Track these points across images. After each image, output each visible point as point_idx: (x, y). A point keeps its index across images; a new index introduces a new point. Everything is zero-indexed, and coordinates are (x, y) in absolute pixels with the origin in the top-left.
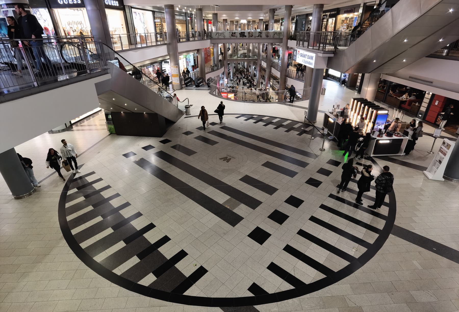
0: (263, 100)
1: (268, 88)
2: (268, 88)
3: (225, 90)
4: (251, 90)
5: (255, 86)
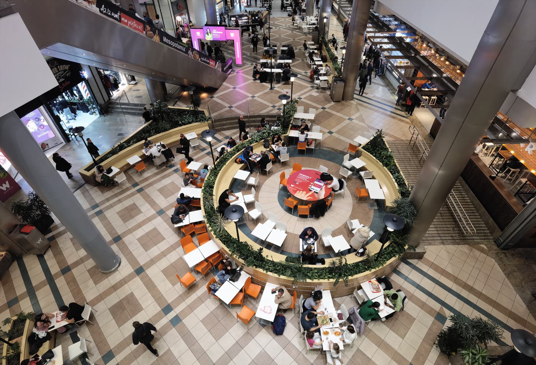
0: (313, 45)
1: (325, 15)
2: (325, 15)
4: (293, 20)
5: (304, 11)
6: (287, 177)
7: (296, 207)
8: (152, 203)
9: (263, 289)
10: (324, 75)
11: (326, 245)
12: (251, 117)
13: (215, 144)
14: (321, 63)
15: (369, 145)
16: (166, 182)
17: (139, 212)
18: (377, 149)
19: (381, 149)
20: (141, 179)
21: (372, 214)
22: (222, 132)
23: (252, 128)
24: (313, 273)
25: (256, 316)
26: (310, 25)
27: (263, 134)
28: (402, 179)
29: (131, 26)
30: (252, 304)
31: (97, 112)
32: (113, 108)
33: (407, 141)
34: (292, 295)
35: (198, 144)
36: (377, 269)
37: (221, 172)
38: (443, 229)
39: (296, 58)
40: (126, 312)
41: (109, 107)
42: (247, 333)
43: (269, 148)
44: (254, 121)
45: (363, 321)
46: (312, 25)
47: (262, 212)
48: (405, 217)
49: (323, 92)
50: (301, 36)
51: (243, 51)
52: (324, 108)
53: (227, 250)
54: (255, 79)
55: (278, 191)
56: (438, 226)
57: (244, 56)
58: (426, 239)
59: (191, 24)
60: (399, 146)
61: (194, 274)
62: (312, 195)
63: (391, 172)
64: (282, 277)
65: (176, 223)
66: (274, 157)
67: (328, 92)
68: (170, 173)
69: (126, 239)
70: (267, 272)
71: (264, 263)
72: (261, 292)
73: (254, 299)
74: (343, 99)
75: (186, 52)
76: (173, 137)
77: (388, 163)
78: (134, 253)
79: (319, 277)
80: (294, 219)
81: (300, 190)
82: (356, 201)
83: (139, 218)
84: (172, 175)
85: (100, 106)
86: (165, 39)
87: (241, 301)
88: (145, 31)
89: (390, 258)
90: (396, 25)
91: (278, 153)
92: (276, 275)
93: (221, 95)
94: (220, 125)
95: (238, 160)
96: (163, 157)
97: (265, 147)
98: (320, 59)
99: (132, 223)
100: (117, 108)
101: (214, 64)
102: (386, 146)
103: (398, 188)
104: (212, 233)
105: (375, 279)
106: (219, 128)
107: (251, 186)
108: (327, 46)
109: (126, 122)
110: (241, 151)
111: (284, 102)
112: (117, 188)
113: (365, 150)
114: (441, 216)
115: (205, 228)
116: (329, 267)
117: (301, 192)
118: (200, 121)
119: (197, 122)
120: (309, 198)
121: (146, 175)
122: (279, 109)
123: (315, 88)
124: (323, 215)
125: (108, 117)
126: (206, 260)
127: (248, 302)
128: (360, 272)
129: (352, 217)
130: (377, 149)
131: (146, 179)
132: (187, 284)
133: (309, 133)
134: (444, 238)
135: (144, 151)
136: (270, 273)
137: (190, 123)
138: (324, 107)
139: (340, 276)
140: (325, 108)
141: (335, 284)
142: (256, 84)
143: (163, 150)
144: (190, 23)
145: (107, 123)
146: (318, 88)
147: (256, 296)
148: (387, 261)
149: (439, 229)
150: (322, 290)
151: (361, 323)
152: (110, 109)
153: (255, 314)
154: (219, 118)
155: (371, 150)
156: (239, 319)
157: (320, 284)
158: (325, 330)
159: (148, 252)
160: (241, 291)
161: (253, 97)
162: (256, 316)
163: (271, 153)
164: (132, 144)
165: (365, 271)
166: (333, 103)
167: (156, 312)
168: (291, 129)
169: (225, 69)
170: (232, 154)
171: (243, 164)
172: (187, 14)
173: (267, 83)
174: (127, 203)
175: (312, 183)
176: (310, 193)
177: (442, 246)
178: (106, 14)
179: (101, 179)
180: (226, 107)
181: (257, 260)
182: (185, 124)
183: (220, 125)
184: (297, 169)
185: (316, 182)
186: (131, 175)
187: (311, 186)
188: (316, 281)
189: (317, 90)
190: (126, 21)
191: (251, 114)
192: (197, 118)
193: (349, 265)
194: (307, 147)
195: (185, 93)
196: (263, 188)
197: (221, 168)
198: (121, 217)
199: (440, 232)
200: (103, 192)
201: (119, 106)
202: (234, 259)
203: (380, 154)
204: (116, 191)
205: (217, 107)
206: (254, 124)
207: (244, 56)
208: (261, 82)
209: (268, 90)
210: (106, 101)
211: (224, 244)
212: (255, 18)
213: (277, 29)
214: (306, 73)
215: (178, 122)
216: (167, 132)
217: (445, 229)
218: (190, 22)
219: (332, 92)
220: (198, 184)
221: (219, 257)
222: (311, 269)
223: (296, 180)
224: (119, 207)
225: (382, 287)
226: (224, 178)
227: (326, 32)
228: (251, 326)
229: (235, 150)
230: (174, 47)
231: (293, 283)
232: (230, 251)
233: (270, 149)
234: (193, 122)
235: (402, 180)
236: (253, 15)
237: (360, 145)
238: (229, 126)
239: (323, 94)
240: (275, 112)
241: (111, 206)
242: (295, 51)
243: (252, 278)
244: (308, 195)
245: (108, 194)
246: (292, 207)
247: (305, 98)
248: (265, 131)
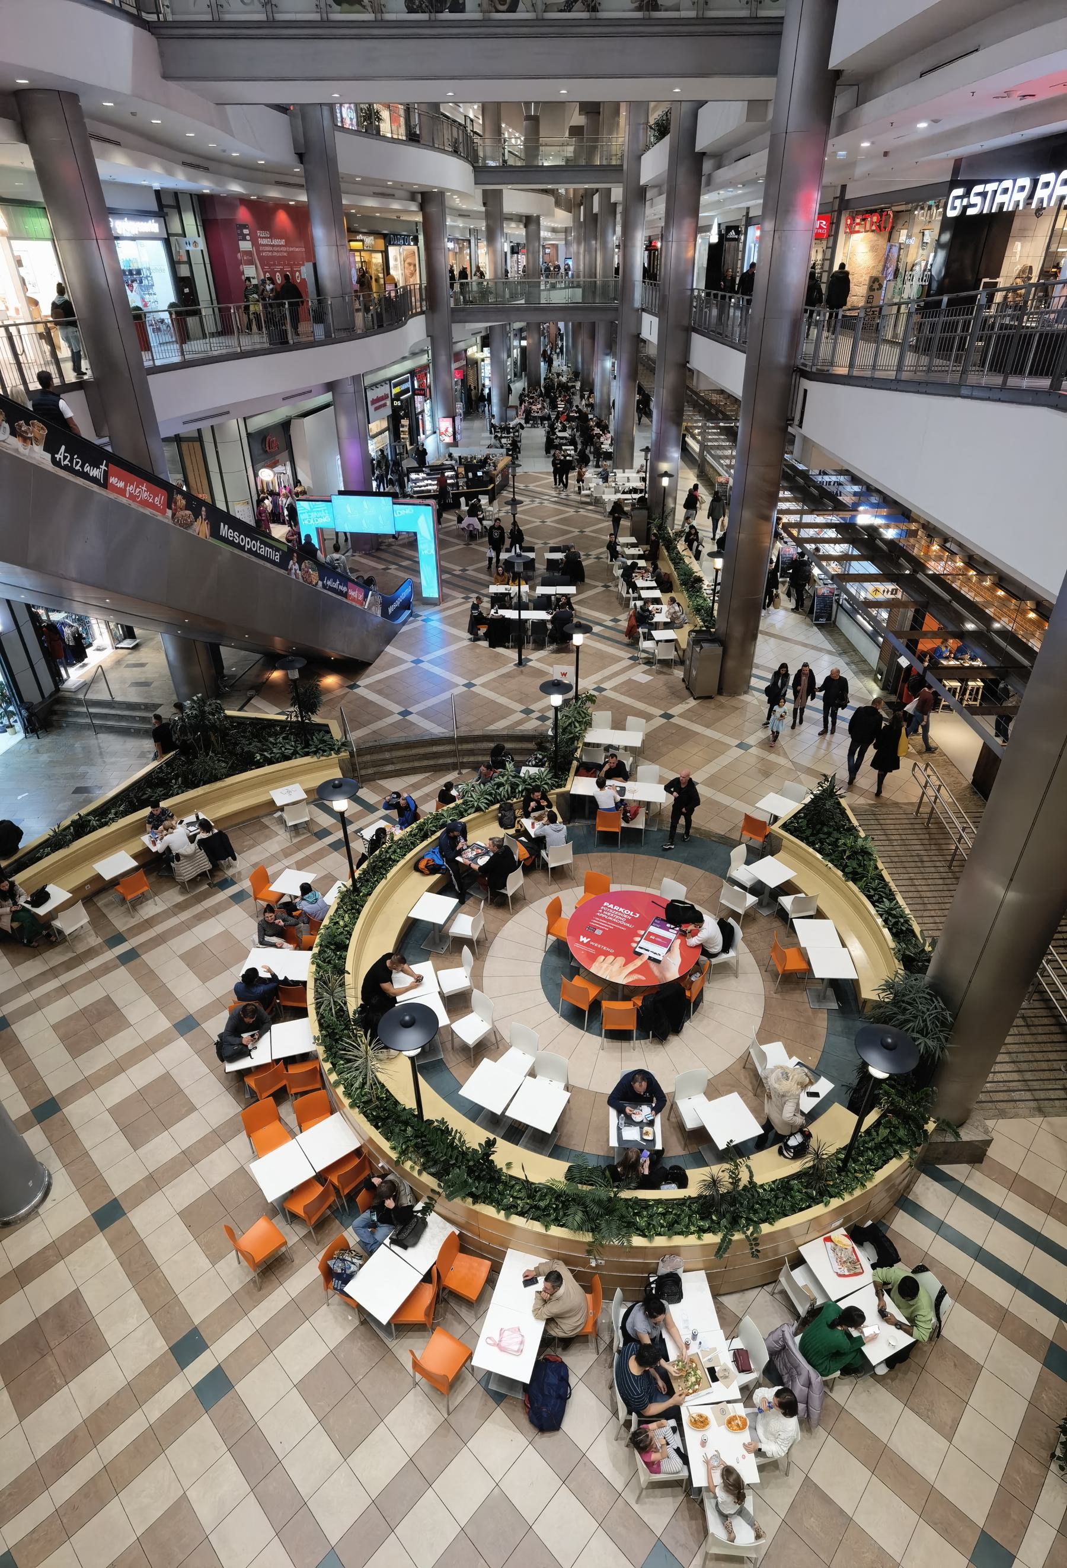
0: (633, 545)
1: (664, 466)
2: (664, 466)
3: (424, 479)
5: (608, 456)
6: (568, 912)
7: (595, 1006)
8: (163, 997)
9: (495, 1270)
10: (667, 626)
11: (690, 1124)
12: (463, 740)
13: (358, 816)
14: (657, 594)
15: (800, 818)
16: (208, 930)
17: (121, 1022)
18: (826, 829)
19: (838, 830)
20: (133, 922)
21: (822, 1023)
22: (381, 782)
23: (464, 771)
24: (651, 1217)
25: (475, 1362)
26: (624, 493)
27: (498, 788)
28: (902, 917)
29: (132, 497)
30: (461, 1321)
31: (18, 726)
32: (65, 714)
33: (911, 807)
34: (588, 1289)
35: (307, 819)
36: (848, 1198)
37: (371, 900)
38: (1035, 1065)
39: (587, 580)
40: (49, 1360)
41: (55, 713)
42: (446, 1426)
43: (513, 826)
44: (472, 753)
45: (816, 1379)
46: (630, 492)
47: (493, 1022)
48: (919, 1032)
49: (665, 673)
50: (599, 521)
51: (443, 563)
52: (667, 716)
53: (385, 1145)
54: (476, 638)
55: (540, 956)
56: (1021, 1057)
57: (445, 576)
58: (988, 1099)
59: (299, 489)
60: (888, 822)
61: (279, 1222)
62: (643, 969)
63: (869, 897)
64: (556, 1231)
65: (232, 1059)
66: (527, 855)
67: (679, 673)
68: (219, 903)
69: (74, 1112)
70: (507, 1216)
71: (500, 1187)
72: (491, 1281)
73: (468, 1303)
74: (720, 692)
75: (283, 564)
76: (235, 798)
77: (860, 870)
78: (95, 1156)
79: (672, 1229)
80: (592, 1043)
81: (606, 954)
82: (773, 987)
83: (120, 1044)
84: (225, 909)
85: (27, 709)
86: (224, 530)
87: (427, 1314)
88: (170, 507)
89: (886, 1162)
90: (855, 494)
91: (538, 843)
92: (537, 1227)
93: (379, 681)
94: (375, 764)
95: (422, 865)
96: (202, 854)
97: (503, 825)
98: (654, 584)
99: (99, 1058)
100: (78, 714)
101: (361, 597)
102: (850, 822)
103: (892, 944)
104: (340, 1090)
105: (842, 1231)
106: (370, 771)
107: (460, 942)
108: (670, 545)
109: (101, 754)
110: (434, 837)
111: (556, 700)
112: (58, 949)
113: (791, 834)
114: (1028, 1026)
115: (318, 1074)
116: (700, 1197)
117: (611, 958)
118: (315, 753)
119: (307, 754)
120: (636, 977)
121: (151, 909)
122: (543, 718)
123: (641, 661)
124: (677, 1029)
125: (47, 741)
126: (321, 1177)
127: (449, 1316)
128: (795, 1209)
129: (766, 1035)
130: (826, 829)
131: (149, 923)
132: (259, 1257)
133: (628, 785)
134: (1042, 1095)
135: (146, 839)
136: (517, 1220)
137: (287, 758)
138: (670, 712)
139: (734, 1223)
140: (672, 716)
141: (721, 1249)
142: (478, 651)
143: (203, 835)
144: (296, 486)
145: (44, 757)
146: (649, 662)
147: (473, 1295)
148: (876, 1170)
149: (1024, 1066)
150: (680, 1272)
151: (809, 1384)
152: (55, 718)
153: (470, 1357)
154: (371, 744)
155: (809, 832)
156: (418, 1376)
157: (674, 1251)
158: (696, 1411)
159: (141, 1151)
160: (427, 1278)
161: (469, 685)
162: (475, 1362)
163: (521, 842)
164: (113, 820)
165: (809, 1207)
166: (692, 703)
167: (149, 1359)
168: (577, 774)
169: (391, 610)
170: (405, 846)
171: (438, 876)
172: (288, 463)
173: (508, 648)
174: (86, 996)
175: (642, 932)
176: (638, 963)
177: (1038, 1120)
178: (69, 469)
179: (12, 920)
180: (391, 713)
181: (478, 1178)
182: (270, 762)
183: (375, 764)
184: (597, 889)
185: (652, 929)
186: (105, 911)
187: (638, 939)
188: (660, 1241)
189: (647, 667)
190: (121, 485)
191: (464, 731)
192: (307, 745)
193: (762, 1186)
194: (624, 824)
195: (276, 675)
196: (499, 948)
197: (373, 889)
198: (63, 1039)
199: (1028, 1076)
200: (14, 964)
201: (84, 710)
202: (405, 1175)
203: (835, 844)
204: (56, 957)
205: (369, 712)
206: (472, 759)
207: (445, 576)
208: (492, 645)
209: (511, 667)
210: (46, 695)
211: (377, 1128)
212: (475, 475)
213: (536, 504)
214: (615, 620)
215: (251, 755)
216: (219, 785)
217: (1044, 1065)
218: (297, 482)
219: (688, 673)
220: (305, 938)
221: (359, 1169)
222: (645, 1204)
223: (594, 923)
224: (60, 1010)
225: (865, 1257)
226: (380, 919)
227: (667, 511)
228: (459, 1399)
229: (415, 835)
230: (250, 551)
231: (591, 1249)
232: (394, 1148)
233: (517, 831)
234: (295, 755)
235: (902, 920)
236: (470, 465)
237: (776, 819)
238: (398, 767)
239: (663, 677)
240: (531, 725)
241: (36, 1006)
242: (584, 563)
243: (461, 1235)
244: (631, 967)
245: (32, 968)
246: (585, 1007)
247: (614, 689)
248: (502, 780)
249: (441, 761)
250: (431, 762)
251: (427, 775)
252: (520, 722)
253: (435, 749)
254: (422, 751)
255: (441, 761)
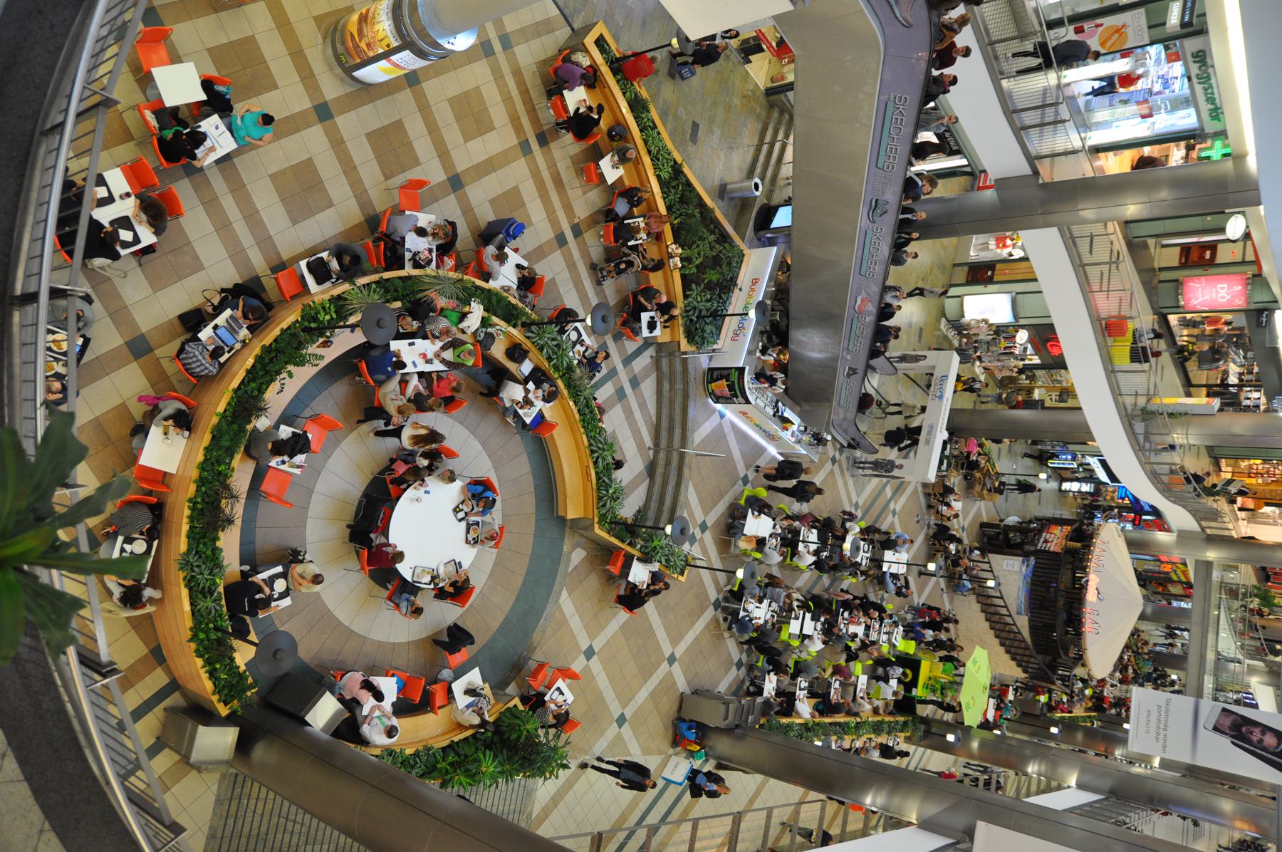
12: (682, 455)
23: (651, 452)
44: (668, 463)
52: (672, 659)
94: (672, 373)
106: (665, 368)
138: (676, 664)
183: (672, 373)
198: (466, 94)
224: (491, 94)
249: (664, 435)
250: (664, 425)
251: (654, 419)
252: (691, 514)
253: (677, 431)
254: (678, 418)
255: (664, 435)
